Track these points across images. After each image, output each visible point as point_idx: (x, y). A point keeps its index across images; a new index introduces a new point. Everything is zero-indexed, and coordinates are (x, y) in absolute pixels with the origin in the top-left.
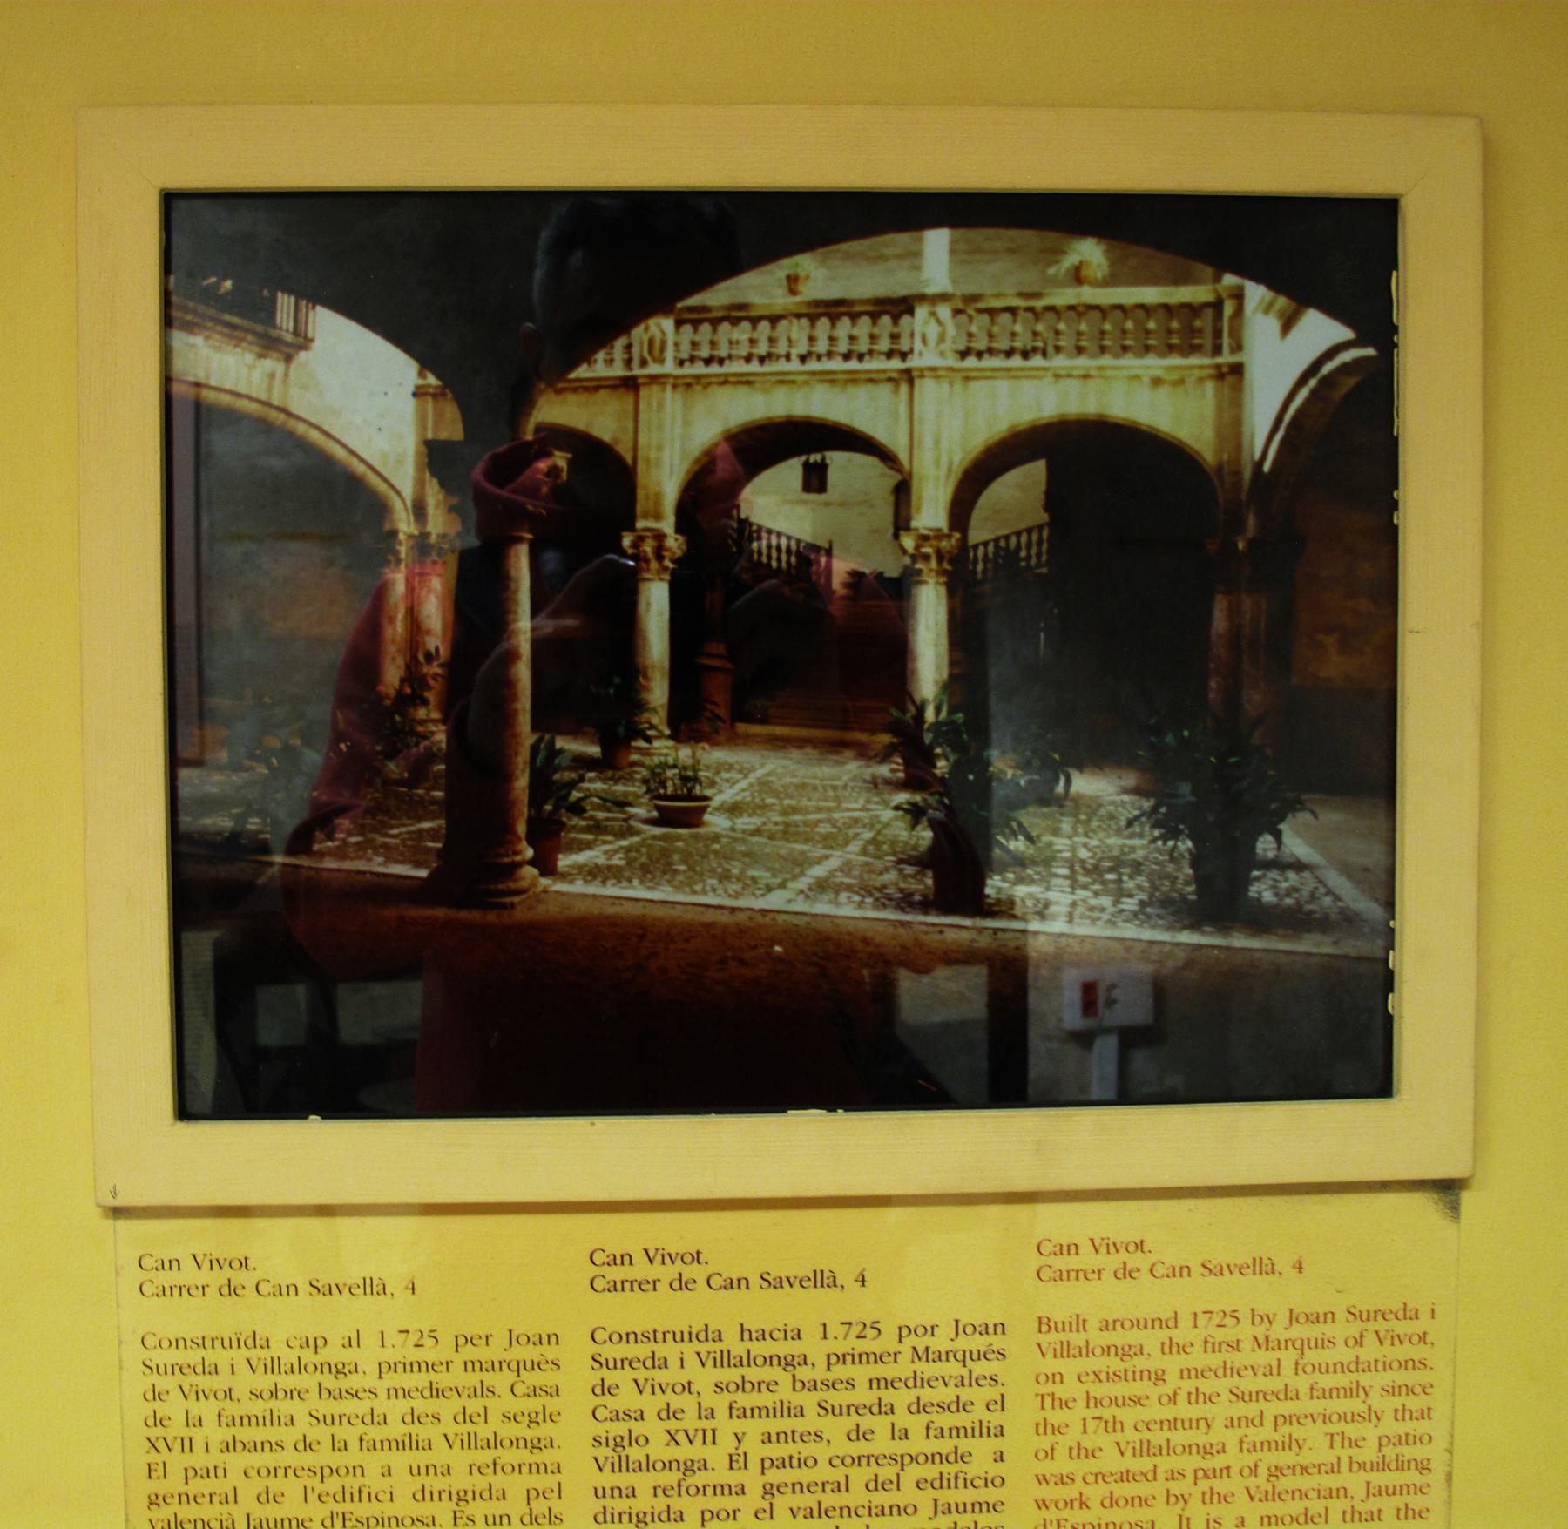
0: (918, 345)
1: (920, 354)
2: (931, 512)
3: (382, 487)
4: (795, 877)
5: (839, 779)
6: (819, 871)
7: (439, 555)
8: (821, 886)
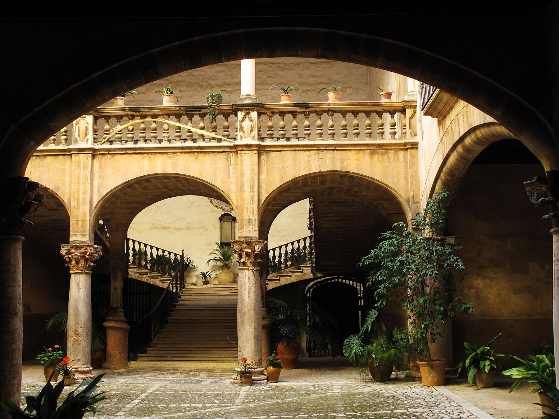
0: (239, 133)
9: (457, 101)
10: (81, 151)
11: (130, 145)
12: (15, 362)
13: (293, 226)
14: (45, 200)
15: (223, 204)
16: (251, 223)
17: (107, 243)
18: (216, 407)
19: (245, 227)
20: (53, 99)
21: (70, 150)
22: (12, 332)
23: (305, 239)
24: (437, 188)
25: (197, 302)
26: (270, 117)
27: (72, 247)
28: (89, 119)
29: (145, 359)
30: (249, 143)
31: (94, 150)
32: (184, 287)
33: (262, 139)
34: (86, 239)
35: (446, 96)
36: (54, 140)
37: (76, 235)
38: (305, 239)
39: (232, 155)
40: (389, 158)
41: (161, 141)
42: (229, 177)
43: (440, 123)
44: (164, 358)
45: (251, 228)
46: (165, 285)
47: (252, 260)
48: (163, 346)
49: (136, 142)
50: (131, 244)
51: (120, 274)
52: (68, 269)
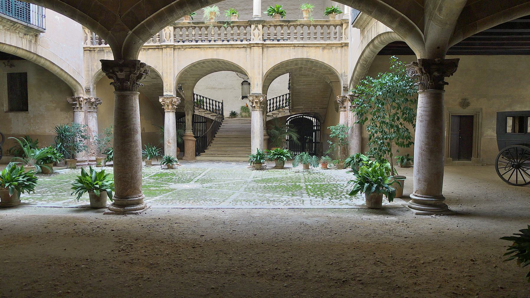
0: (252, 37)
1: (253, 39)
2: (257, 88)
3: (74, 83)
8: (236, 201)
9: (371, 19)
10: (167, 46)
11: (194, 43)
13: (281, 86)
14: (149, 73)
15: (243, 76)
17: (183, 96)
20: (151, 17)
21: (161, 46)
22: (136, 142)
23: (286, 95)
24: (358, 68)
25: (231, 127)
26: (269, 28)
27: (165, 98)
28: (171, 28)
30: (257, 42)
31: (175, 46)
32: (223, 119)
33: (265, 40)
34: (172, 94)
35: (365, 16)
36: (153, 40)
38: (286, 95)
39: (248, 49)
40: (332, 51)
41: (210, 41)
43: (362, 32)
46: (213, 118)
47: (259, 105)
49: (197, 41)
50: (195, 96)
51: (190, 112)
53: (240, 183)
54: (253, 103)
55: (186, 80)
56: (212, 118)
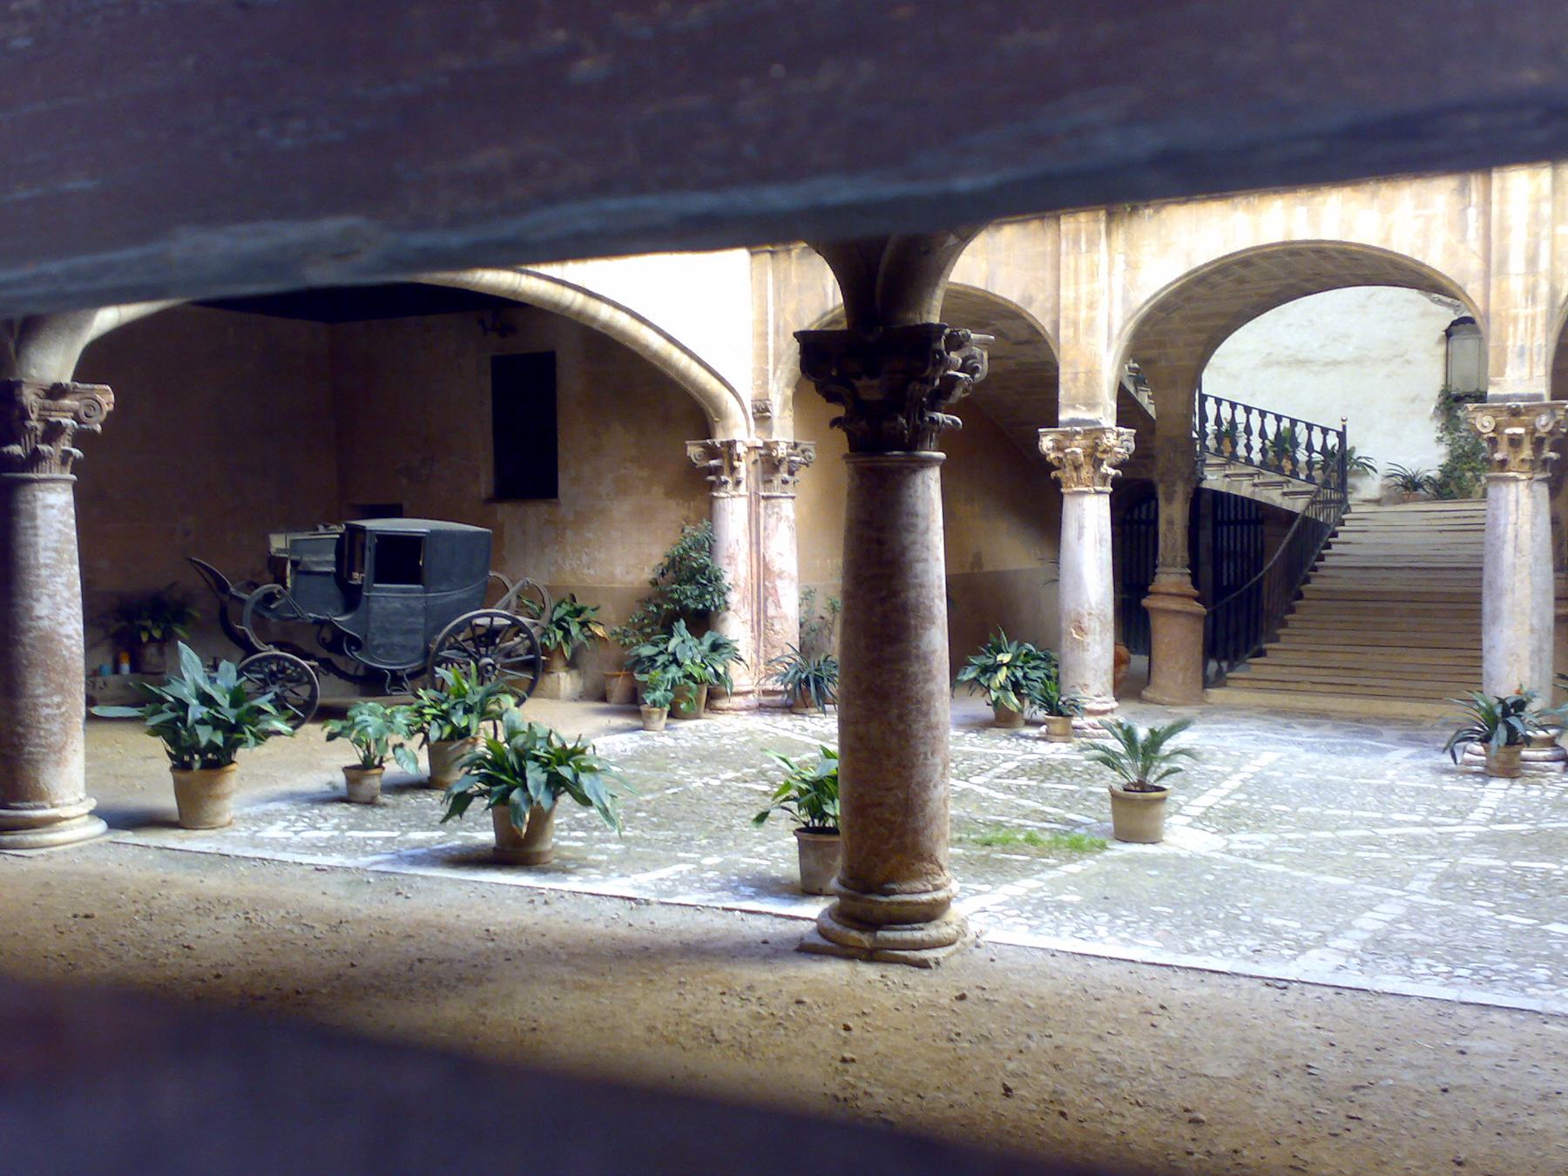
4: (1337, 933)
5: (1382, 776)
6: (1370, 922)
7: (791, 473)
12: (934, 719)
16: (1527, 356)
18: (1416, 824)
19: (1508, 370)
22: (924, 658)
27: (1065, 434)
29: (1246, 684)
37: (1074, 407)
42: (1463, 240)
44: (1291, 686)
45: (1526, 371)
48: (1291, 655)
52: (1057, 483)
53: (1416, 844)
54: (1493, 442)
55: (1161, 344)
56: (1286, 504)
